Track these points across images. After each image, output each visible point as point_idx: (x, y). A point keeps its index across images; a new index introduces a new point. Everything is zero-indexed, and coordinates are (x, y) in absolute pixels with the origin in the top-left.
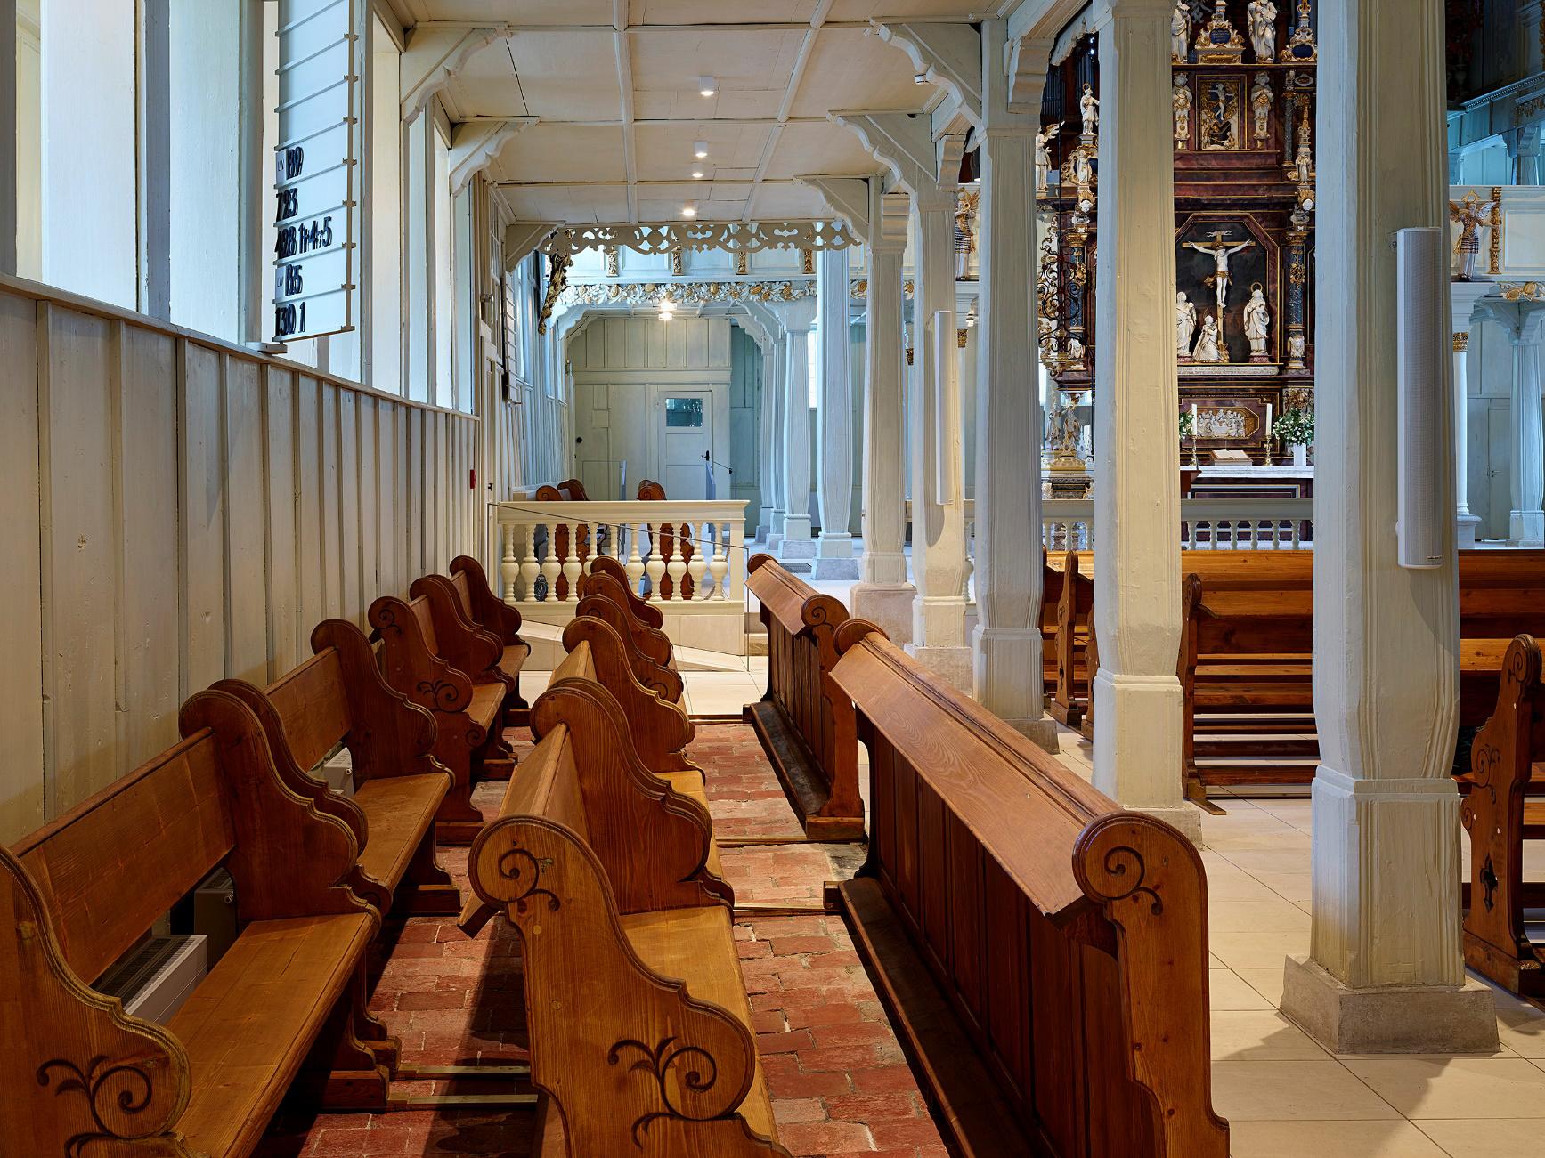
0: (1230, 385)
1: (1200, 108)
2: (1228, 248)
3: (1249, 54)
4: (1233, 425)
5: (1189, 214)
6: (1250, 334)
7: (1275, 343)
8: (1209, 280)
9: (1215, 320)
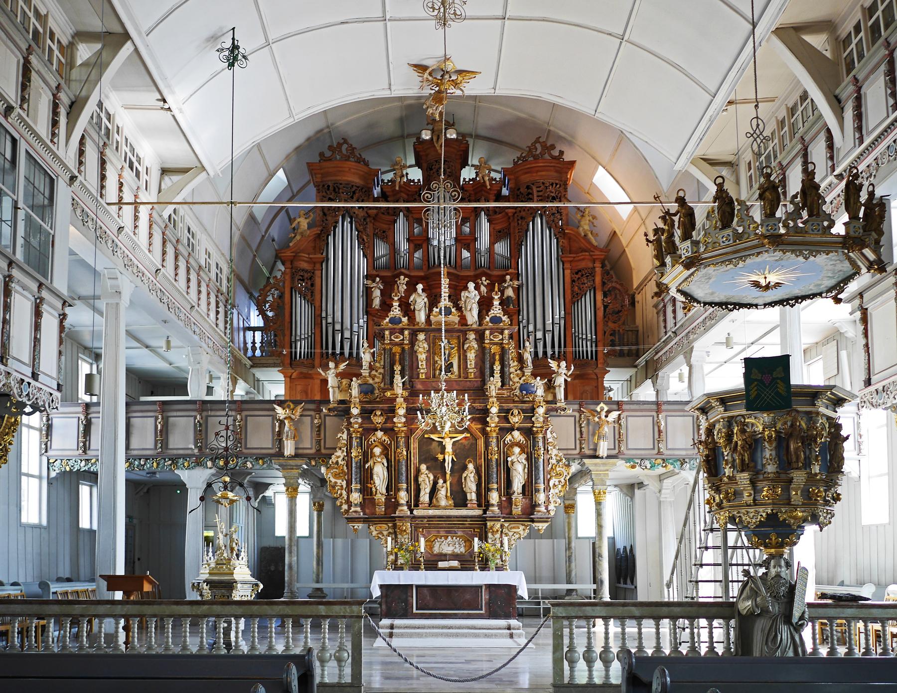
1: (435, 354)
3: (463, 320)
4: (457, 546)
7: (482, 495)
8: (440, 457)
9: (445, 482)
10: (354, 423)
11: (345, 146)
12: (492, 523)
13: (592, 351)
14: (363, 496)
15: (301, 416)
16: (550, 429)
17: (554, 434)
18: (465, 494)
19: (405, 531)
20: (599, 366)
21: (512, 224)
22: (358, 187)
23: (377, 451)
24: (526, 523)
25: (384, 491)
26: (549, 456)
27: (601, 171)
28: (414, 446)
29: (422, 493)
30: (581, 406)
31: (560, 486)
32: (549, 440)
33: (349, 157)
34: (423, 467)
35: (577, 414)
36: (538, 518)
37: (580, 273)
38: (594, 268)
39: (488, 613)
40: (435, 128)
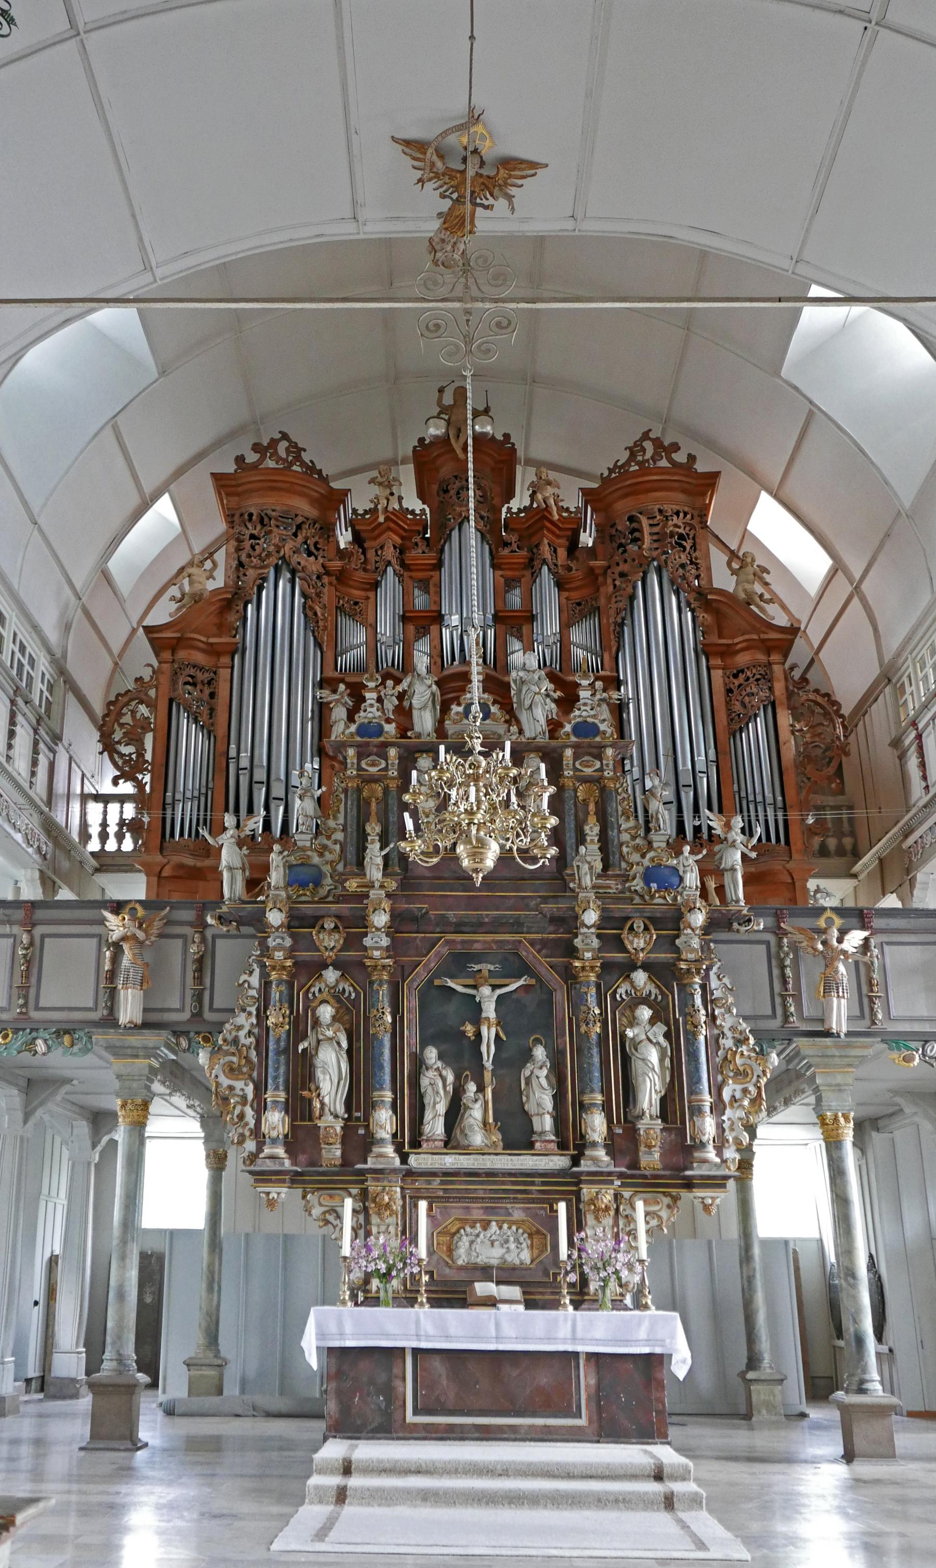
0: (503, 1183)
2: (494, 987)
5: (441, 938)
6: (530, 1107)
8: (469, 1029)
9: (481, 1089)
10: (277, 948)
11: (283, 445)
12: (594, 1189)
13: (776, 821)
14: (293, 1120)
15: (161, 936)
16: (715, 969)
17: (726, 980)
18: (527, 1118)
19: (388, 1206)
20: (795, 856)
21: (602, 590)
22: (308, 519)
23: (326, 1012)
24: (674, 1191)
25: (340, 1109)
26: (716, 1032)
27: (766, 502)
28: (411, 1003)
29: (428, 1115)
30: (778, 916)
31: (746, 1103)
32: (717, 994)
33: (291, 464)
34: (431, 1054)
35: (771, 938)
36: (702, 1177)
37: (742, 677)
38: (770, 664)
39: (596, 1425)
40: (453, 418)
